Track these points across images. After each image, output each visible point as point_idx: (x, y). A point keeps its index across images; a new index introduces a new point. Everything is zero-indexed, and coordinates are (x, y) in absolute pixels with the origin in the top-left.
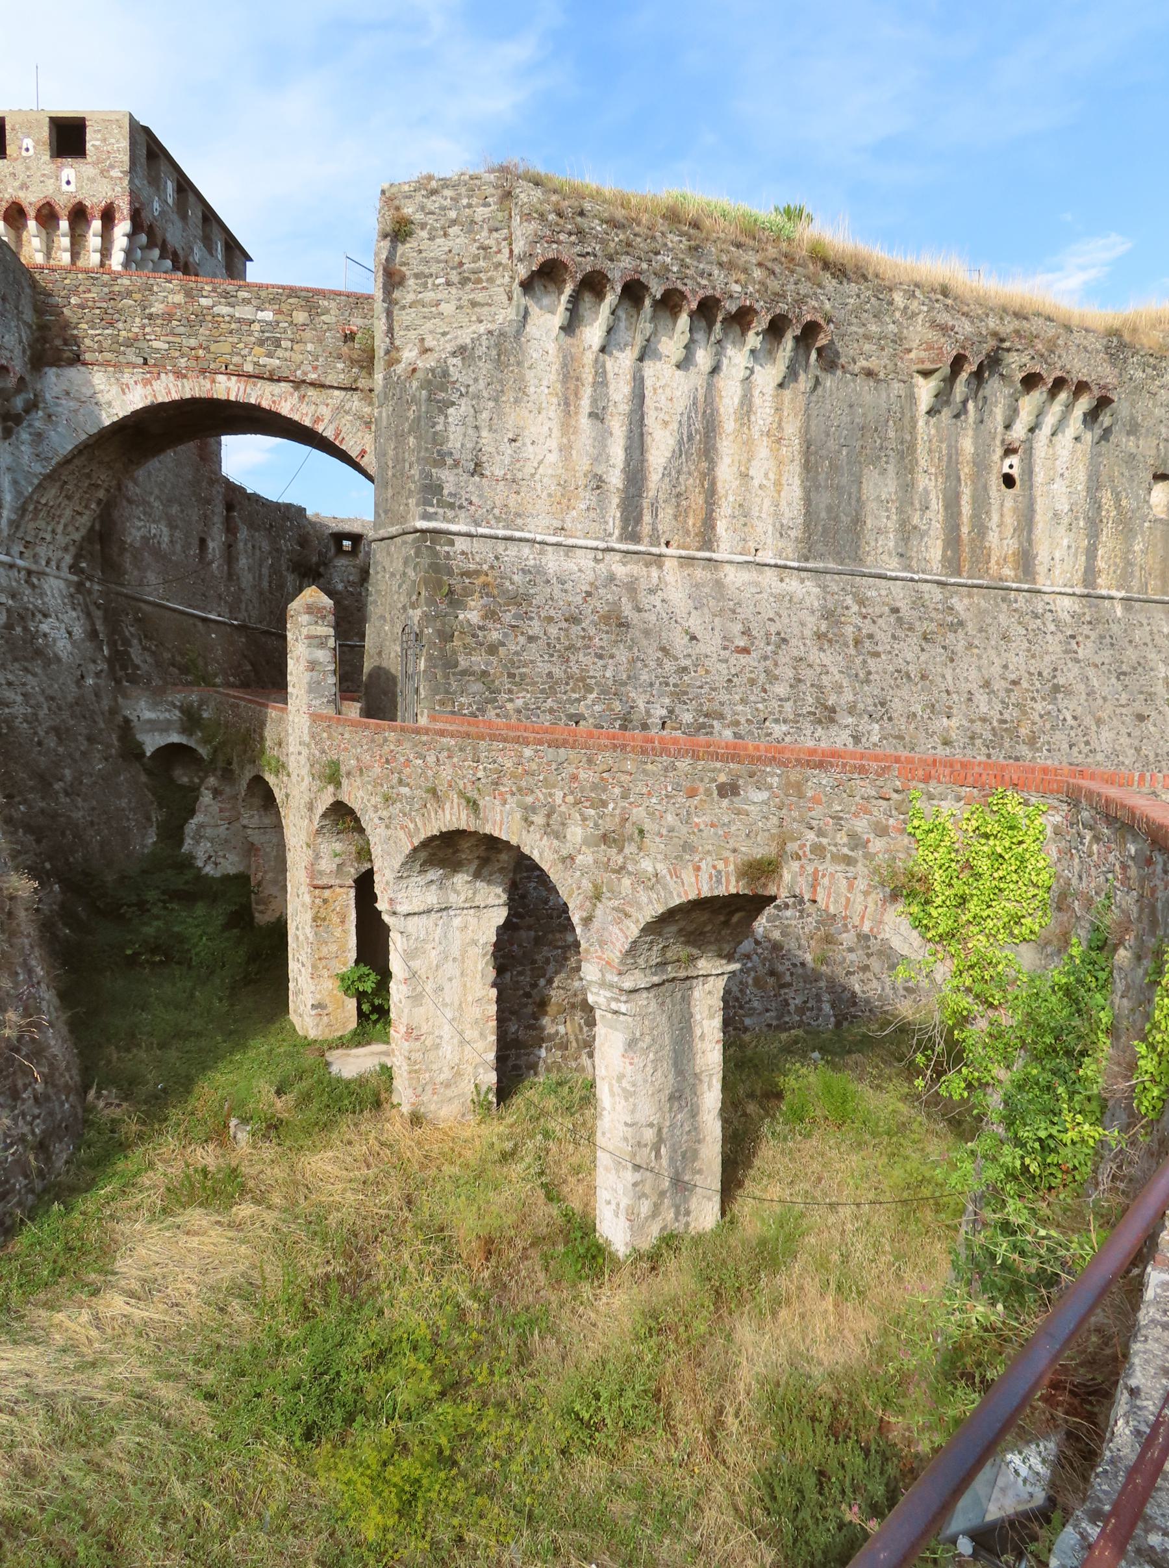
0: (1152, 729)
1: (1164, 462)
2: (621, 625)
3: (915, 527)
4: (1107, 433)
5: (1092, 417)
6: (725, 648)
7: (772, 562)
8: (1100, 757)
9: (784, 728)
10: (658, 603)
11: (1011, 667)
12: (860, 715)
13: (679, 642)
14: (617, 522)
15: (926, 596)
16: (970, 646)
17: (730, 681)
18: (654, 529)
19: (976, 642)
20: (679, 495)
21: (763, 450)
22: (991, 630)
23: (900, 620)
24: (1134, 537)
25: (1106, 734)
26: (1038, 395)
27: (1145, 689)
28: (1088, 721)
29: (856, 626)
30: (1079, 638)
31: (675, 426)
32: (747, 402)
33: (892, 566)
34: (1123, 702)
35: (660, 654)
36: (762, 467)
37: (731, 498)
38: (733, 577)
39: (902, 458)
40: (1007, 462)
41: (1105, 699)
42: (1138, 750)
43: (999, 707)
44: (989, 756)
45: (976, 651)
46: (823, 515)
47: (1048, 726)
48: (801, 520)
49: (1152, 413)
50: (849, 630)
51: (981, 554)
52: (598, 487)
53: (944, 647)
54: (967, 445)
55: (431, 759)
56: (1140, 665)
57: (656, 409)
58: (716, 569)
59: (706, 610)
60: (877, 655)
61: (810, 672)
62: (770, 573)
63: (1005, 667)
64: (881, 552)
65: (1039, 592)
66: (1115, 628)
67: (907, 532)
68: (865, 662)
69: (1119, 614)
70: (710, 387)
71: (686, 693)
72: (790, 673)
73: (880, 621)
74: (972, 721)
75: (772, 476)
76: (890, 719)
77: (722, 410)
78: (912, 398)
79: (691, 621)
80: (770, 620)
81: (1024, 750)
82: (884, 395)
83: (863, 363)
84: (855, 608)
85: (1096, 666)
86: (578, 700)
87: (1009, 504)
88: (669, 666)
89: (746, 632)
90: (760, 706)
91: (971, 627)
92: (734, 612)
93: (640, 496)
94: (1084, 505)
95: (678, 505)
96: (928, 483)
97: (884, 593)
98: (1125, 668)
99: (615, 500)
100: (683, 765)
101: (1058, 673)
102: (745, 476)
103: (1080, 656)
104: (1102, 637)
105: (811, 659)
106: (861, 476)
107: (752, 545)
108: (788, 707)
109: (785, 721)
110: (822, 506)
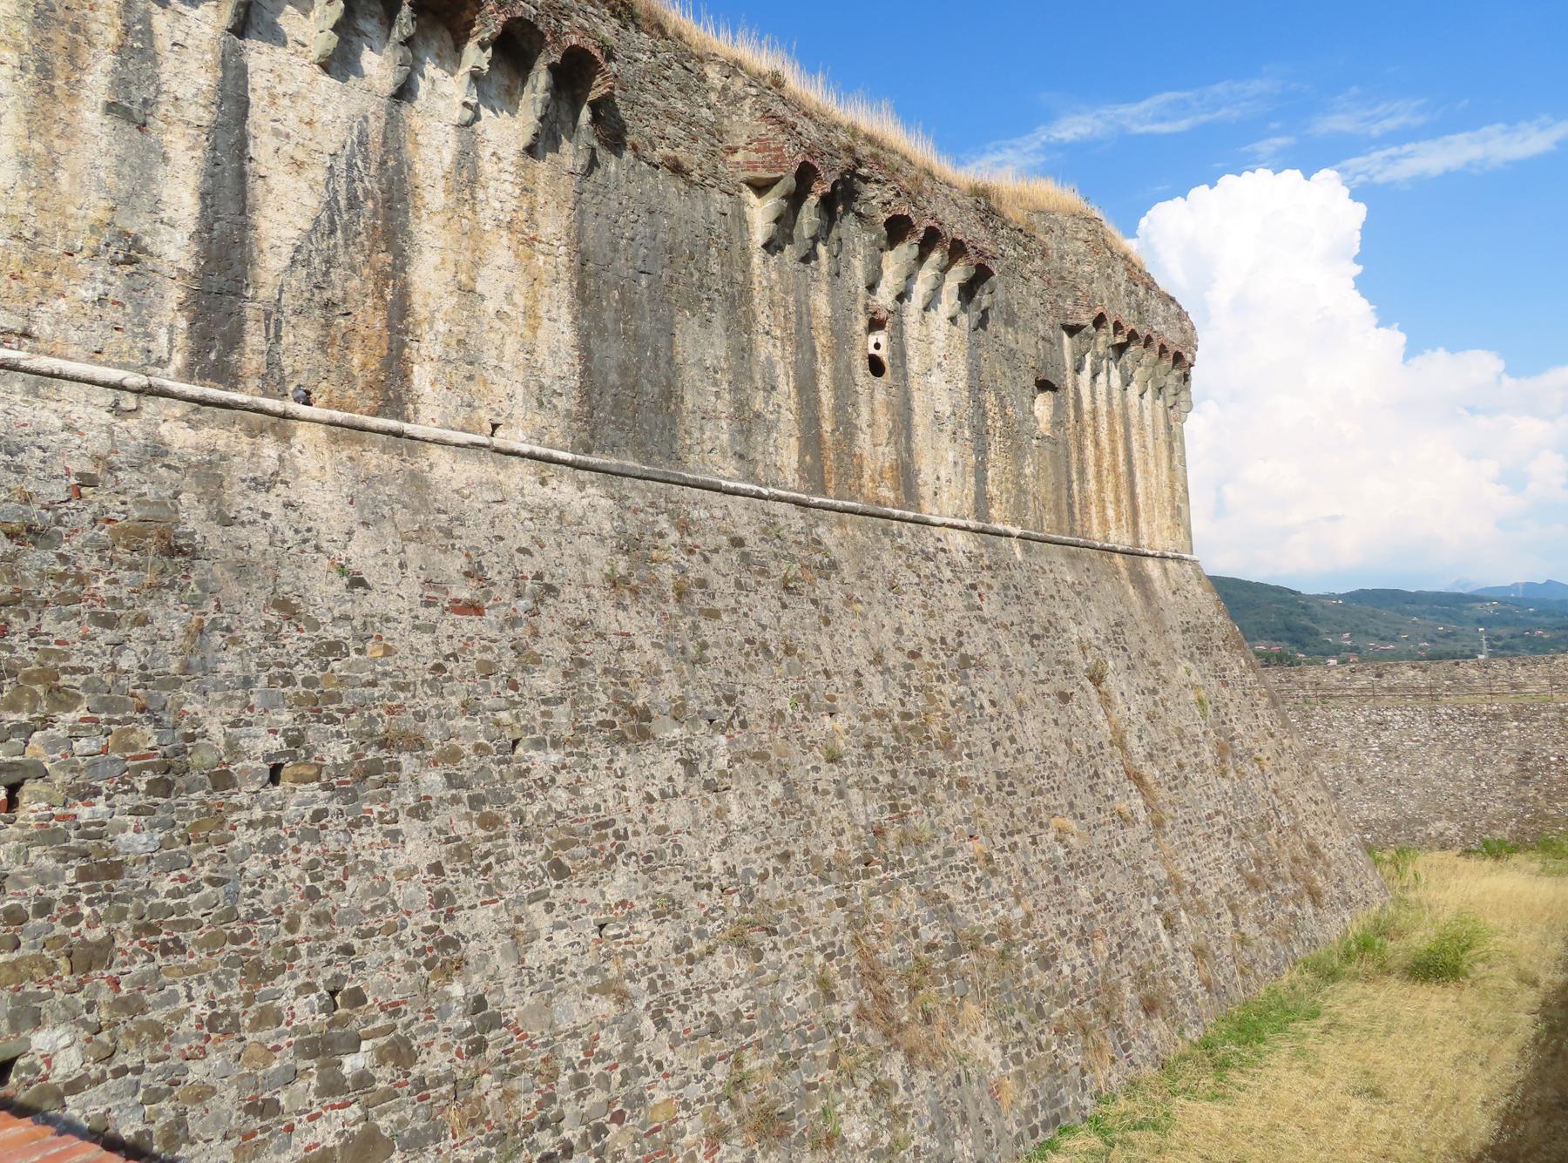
0: (1078, 712)
1: (1044, 367)
2: (172, 551)
3: (758, 415)
4: (983, 322)
5: (967, 292)
6: (429, 603)
7: (525, 448)
8: (1030, 759)
9: (555, 757)
10: (275, 510)
11: (907, 632)
12: (694, 721)
13: (321, 590)
14: (180, 340)
15: (782, 522)
16: (849, 600)
17: (438, 668)
18: (272, 364)
19: (857, 594)
20: (328, 305)
21: (501, 251)
22: (875, 576)
23: (745, 557)
24: (1024, 457)
25: (1032, 725)
26: (906, 251)
27: (1062, 657)
28: (1009, 707)
29: (677, 566)
30: (982, 589)
31: (321, 175)
32: (467, 159)
33: (727, 472)
34: (1042, 676)
35: (273, 616)
36: (499, 278)
37: (441, 327)
38: (445, 469)
39: (732, 305)
40: (872, 339)
41: (1021, 672)
42: (1069, 744)
43: (898, 693)
44: (894, 773)
45: (859, 607)
46: (613, 377)
47: (964, 719)
48: (574, 382)
49: (1027, 302)
50: (666, 573)
51: (850, 465)
52: (129, 261)
53: (814, 602)
54: (821, 303)
56: (1051, 624)
57: (276, 133)
58: (412, 452)
59: (387, 528)
60: (713, 614)
61: (599, 647)
62: (519, 467)
63: (899, 631)
64: (710, 448)
65: (927, 523)
66: (1018, 576)
67: (747, 423)
68: (695, 627)
69: (1019, 556)
70: (393, 122)
71: (335, 698)
72: (563, 650)
73: (715, 558)
74: (865, 719)
75: (518, 298)
76: (744, 724)
77: (419, 167)
78: (741, 219)
79: (354, 549)
80: (522, 550)
81: (938, 759)
82: (700, 207)
83: (663, 150)
84: (674, 536)
85: (1005, 627)
86: (27, 730)
87: (880, 396)
88: (294, 640)
89: (474, 573)
90: (504, 716)
91: (847, 570)
92: (449, 534)
93: (238, 294)
94: (966, 410)
95: (328, 325)
96: (771, 350)
97: (718, 513)
98: (1037, 630)
99: (175, 294)
101: (964, 639)
102: (467, 291)
103: (986, 613)
104: (1006, 587)
105: (602, 622)
106: (672, 324)
107: (485, 416)
108: (562, 714)
109: (555, 744)
110: (611, 363)
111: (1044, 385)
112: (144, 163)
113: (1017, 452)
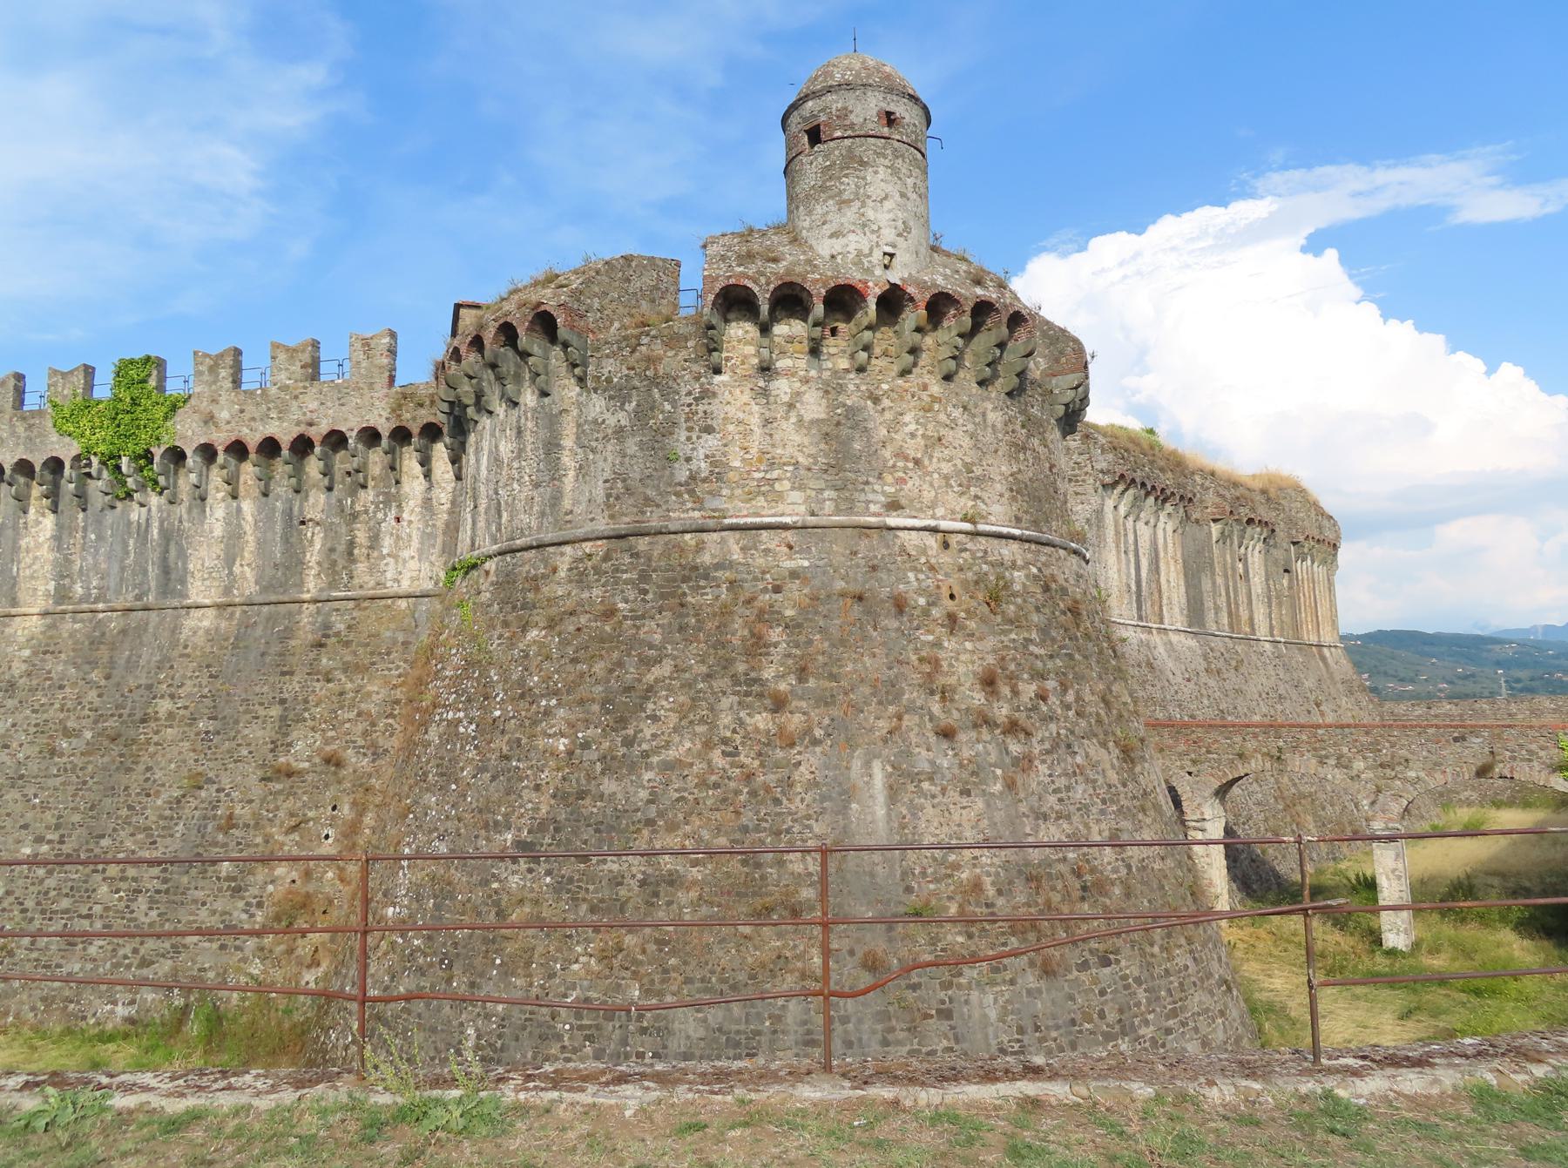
36: (1173, 575)
55: (1238, 739)
67: (1217, 609)
100: (1431, 731)
111: (1286, 571)
112: (1128, 561)
113: (1280, 604)
